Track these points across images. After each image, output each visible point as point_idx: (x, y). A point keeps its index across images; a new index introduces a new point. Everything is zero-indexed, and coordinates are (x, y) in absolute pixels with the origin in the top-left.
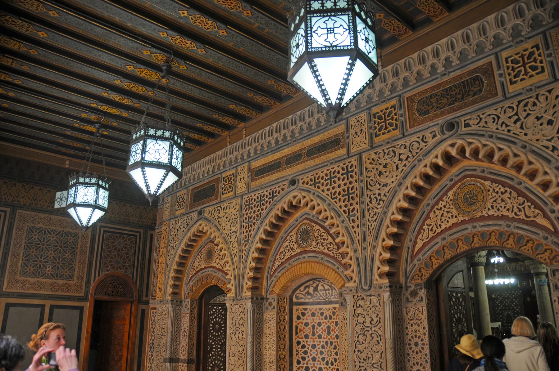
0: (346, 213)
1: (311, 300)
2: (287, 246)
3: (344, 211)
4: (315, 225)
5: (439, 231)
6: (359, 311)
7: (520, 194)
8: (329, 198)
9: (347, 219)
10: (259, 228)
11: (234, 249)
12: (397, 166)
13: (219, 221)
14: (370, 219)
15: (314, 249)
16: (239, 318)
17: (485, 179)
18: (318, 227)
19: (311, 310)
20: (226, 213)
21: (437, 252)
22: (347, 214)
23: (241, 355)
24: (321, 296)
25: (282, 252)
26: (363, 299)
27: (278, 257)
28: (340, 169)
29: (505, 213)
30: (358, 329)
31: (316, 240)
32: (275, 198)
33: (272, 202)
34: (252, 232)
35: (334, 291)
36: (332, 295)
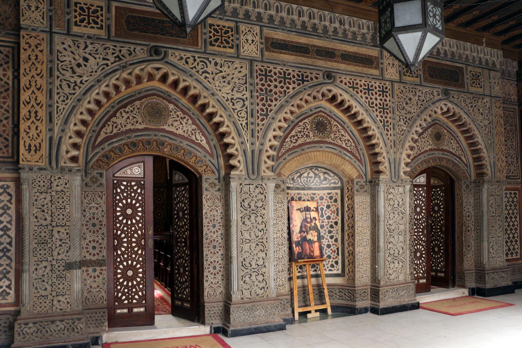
0: (381, 122)
1: (292, 186)
2: (300, 132)
3: (380, 120)
4: (333, 120)
5: (423, 151)
7: (458, 143)
8: (367, 105)
9: (383, 128)
10: (282, 106)
11: (241, 119)
12: (417, 103)
13: (206, 78)
14: (399, 132)
15: (332, 142)
17: (445, 129)
18: (336, 123)
20: (221, 72)
21: (420, 163)
22: (383, 123)
24: (301, 182)
25: (294, 136)
26: (393, 188)
27: (288, 139)
28: (377, 85)
29: (452, 150)
31: (335, 134)
32: (306, 83)
33: (302, 85)
34: (272, 108)
35: (317, 179)
36: (313, 182)
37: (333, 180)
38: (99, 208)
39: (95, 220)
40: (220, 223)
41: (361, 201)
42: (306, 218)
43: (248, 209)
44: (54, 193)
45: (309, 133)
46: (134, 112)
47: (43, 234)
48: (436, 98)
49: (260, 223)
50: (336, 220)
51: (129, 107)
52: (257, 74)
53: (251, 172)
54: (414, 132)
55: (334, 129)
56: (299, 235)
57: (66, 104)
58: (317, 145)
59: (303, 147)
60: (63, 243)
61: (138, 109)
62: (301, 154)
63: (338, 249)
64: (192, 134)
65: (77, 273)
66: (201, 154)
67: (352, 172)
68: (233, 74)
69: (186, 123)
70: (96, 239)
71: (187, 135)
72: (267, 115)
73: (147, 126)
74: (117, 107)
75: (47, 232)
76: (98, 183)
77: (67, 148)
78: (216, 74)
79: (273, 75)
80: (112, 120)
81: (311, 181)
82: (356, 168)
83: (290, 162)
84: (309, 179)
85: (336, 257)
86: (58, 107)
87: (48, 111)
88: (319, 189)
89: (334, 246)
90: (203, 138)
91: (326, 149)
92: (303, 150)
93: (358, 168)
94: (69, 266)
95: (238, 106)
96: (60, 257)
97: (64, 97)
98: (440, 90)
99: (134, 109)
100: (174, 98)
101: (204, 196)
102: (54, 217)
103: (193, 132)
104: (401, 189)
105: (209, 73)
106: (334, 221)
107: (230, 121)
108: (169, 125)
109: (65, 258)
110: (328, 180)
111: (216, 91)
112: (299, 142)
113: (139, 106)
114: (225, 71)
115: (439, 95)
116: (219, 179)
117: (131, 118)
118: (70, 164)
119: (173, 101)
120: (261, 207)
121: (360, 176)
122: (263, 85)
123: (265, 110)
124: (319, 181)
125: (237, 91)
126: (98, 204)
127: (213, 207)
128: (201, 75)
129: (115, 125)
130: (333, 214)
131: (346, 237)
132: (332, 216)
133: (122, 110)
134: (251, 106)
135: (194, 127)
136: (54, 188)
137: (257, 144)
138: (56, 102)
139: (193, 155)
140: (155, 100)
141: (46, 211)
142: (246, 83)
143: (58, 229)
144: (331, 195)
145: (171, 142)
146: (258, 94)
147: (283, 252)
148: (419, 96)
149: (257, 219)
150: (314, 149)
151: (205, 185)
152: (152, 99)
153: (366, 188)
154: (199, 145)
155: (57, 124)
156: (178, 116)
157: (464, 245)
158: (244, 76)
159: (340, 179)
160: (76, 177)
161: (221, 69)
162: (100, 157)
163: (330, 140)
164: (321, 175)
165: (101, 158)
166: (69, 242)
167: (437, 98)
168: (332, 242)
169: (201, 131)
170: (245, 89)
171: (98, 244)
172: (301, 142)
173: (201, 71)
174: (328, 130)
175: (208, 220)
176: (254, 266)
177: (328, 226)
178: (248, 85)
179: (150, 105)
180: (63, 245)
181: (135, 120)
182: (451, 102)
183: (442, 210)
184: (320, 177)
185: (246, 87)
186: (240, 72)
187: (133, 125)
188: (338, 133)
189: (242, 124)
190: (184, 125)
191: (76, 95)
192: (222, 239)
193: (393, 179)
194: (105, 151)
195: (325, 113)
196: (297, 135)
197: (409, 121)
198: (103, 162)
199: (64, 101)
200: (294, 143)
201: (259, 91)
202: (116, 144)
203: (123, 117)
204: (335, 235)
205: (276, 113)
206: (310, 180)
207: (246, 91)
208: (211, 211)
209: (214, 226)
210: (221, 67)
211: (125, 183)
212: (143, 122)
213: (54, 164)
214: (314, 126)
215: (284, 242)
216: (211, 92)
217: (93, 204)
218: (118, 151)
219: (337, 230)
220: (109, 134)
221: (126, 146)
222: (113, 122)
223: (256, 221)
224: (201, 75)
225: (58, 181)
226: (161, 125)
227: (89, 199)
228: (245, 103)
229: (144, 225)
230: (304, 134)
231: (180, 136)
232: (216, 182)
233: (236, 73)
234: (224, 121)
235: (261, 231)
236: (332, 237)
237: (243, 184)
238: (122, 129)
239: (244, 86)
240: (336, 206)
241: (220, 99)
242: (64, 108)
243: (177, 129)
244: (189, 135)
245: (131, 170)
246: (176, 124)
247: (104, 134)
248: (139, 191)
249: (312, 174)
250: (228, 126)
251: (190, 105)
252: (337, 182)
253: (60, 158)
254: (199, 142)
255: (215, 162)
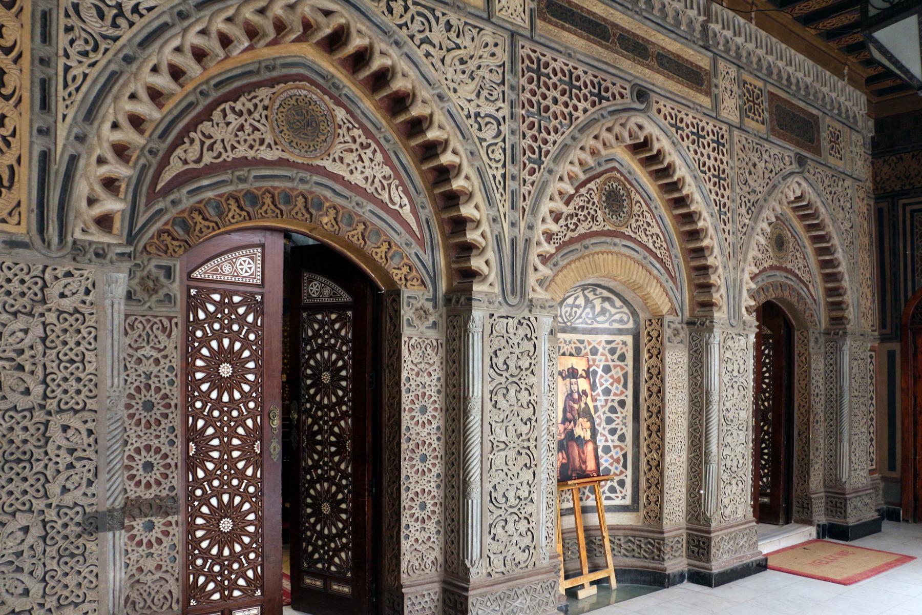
2: (582, 208)
4: (634, 191)
6: (728, 354)
10: (565, 148)
11: (494, 165)
13: (428, 55)
15: (633, 235)
16: (517, 351)
18: (638, 197)
19: (589, 343)
20: (458, 47)
23: (526, 444)
24: (561, 316)
29: (797, 271)
30: (726, 379)
31: (637, 221)
35: (588, 310)
36: (580, 317)
37: (618, 316)
38: (162, 361)
39: (152, 392)
40: (435, 402)
41: (676, 360)
42: (572, 391)
43: (505, 374)
44: (51, 318)
45: (596, 211)
46: (256, 115)
47: (19, 435)
48: (788, 168)
49: (525, 405)
50: (622, 397)
51: (242, 99)
52: (524, 66)
53: (509, 288)
54: (759, 230)
55: (636, 209)
56: (561, 427)
57: (93, 65)
58: (608, 240)
59: (587, 242)
60: (80, 459)
61: (266, 108)
62: (583, 257)
63: (625, 456)
64: (383, 188)
65: (114, 541)
66: (400, 238)
67: (661, 301)
68: (480, 57)
69: (372, 160)
70: (155, 443)
71: (373, 190)
72: (540, 162)
73: (286, 156)
74: (215, 95)
75: (32, 430)
76: (161, 293)
77: (92, 190)
78: (449, 50)
79: (552, 75)
80: (200, 127)
81: (578, 315)
82: (667, 294)
83: (565, 271)
84: (574, 309)
85: (622, 472)
86: (67, 68)
87: (39, 75)
88: (591, 332)
89: (618, 449)
90: (405, 200)
91: (623, 250)
92: (586, 248)
93: (671, 293)
94: (95, 524)
95: (489, 133)
96: (68, 499)
97: (86, 42)
98: (792, 155)
99: (256, 106)
100: (346, 95)
101: (404, 338)
102: (53, 386)
103: (385, 183)
104: (743, 340)
105: (434, 46)
106: (618, 398)
107: (472, 165)
108: (334, 160)
109: (83, 501)
110: (607, 314)
111: (447, 91)
112: (581, 230)
113: (267, 102)
114: (465, 48)
115: (791, 164)
116: (434, 299)
117: (248, 129)
118: (98, 237)
119: (344, 100)
120: (527, 369)
121: (673, 311)
122: (534, 93)
123: (537, 150)
124: (591, 316)
125: (487, 99)
126: (160, 351)
127: (422, 366)
128: (419, 47)
129: (208, 142)
130: (615, 385)
131: (644, 433)
132: (613, 389)
133: (226, 106)
134: (512, 137)
135: (387, 171)
136: (54, 302)
137: (523, 224)
138: (61, 52)
139: (383, 238)
140: (305, 92)
141: (27, 368)
142: (503, 83)
143: (65, 419)
144: (613, 345)
145: (339, 201)
146: (523, 112)
147: (550, 467)
148: (766, 162)
149: (520, 396)
150: (603, 248)
151: (407, 313)
152: (297, 88)
153: (682, 335)
154: (397, 215)
155: (64, 116)
156: (354, 141)
157: (811, 448)
158: (500, 66)
159: (634, 313)
160: (114, 275)
161: (458, 41)
162: (166, 224)
163: (628, 232)
164: (597, 303)
165: (169, 227)
166: (93, 457)
167: (789, 169)
168: (613, 441)
169: (402, 183)
170: (501, 95)
171: (158, 456)
172: (583, 231)
173: (419, 36)
174: (625, 210)
175: (411, 396)
176: (513, 501)
177: (606, 409)
178: (506, 88)
179: (293, 102)
180: (78, 465)
181: (257, 135)
182: (806, 179)
183: (767, 381)
184: (593, 307)
185: (503, 92)
186: (493, 55)
187: (251, 147)
188: (641, 218)
189: (494, 177)
190: (367, 163)
191: (120, 43)
192: (439, 439)
193: (732, 321)
194: (180, 208)
195: (622, 174)
196: (577, 215)
197: (753, 208)
198: (174, 239)
199: (85, 54)
200: (573, 231)
201: (526, 104)
202: (210, 194)
203: (228, 124)
204: (619, 427)
205: (556, 160)
206: (576, 312)
207: (504, 101)
208: (417, 375)
209: (424, 410)
210: (458, 36)
211: (217, 297)
212: (276, 144)
213: (52, 231)
214: (604, 198)
215: (552, 446)
216: (436, 92)
217: (147, 351)
218: (212, 212)
219: (625, 418)
220: (192, 166)
221: (232, 202)
222: (203, 134)
223: (518, 400)
224: (419, 47)
225: (64, 281)
226: (316, 157)
227: (136, 336)
228: (502, 128)
229: (260, 404)
230: (589, 213)
231: (355, 188)
232: (429, 306)
233: (485, 55)
234: (460, 165)
235: (526, 424)
236: (613, 432)
237: (495, 316)
238: (224, 156)
239: (500, 89)
240: (622, 368)
241: (454, 111)
242: (85, 76)
243: (351, 172)
244: (376, 189)
245: (232, 264)
246: (349, 158)
247: (180, 163)
248: (250, 318)
249: (581, 301)
250: (467, 178)
251: (379, 116)
252: (626, 319)
253: (72, 215)
254: (397, 207)
255: (427, 259)
